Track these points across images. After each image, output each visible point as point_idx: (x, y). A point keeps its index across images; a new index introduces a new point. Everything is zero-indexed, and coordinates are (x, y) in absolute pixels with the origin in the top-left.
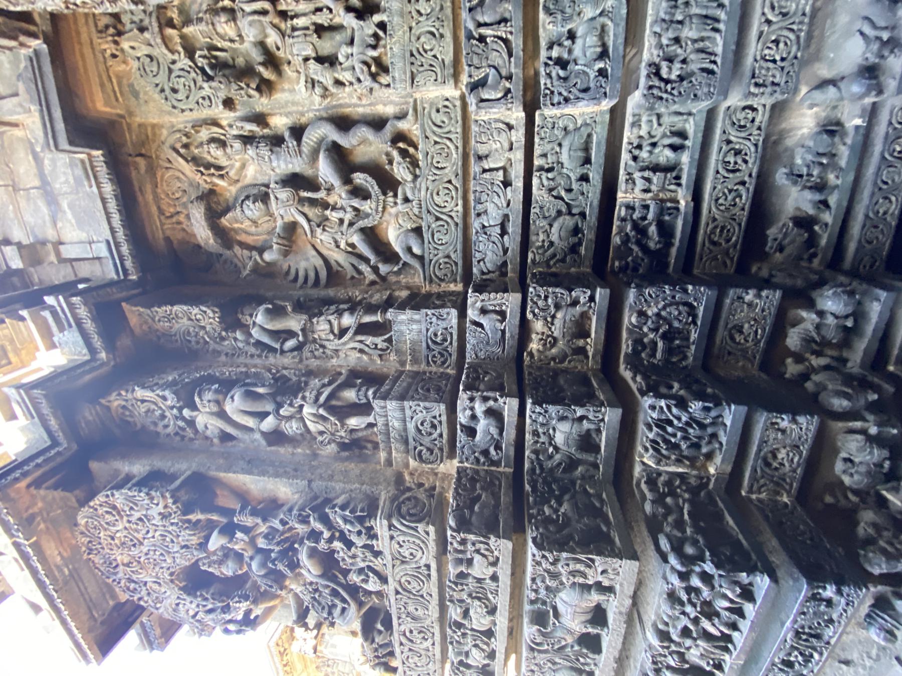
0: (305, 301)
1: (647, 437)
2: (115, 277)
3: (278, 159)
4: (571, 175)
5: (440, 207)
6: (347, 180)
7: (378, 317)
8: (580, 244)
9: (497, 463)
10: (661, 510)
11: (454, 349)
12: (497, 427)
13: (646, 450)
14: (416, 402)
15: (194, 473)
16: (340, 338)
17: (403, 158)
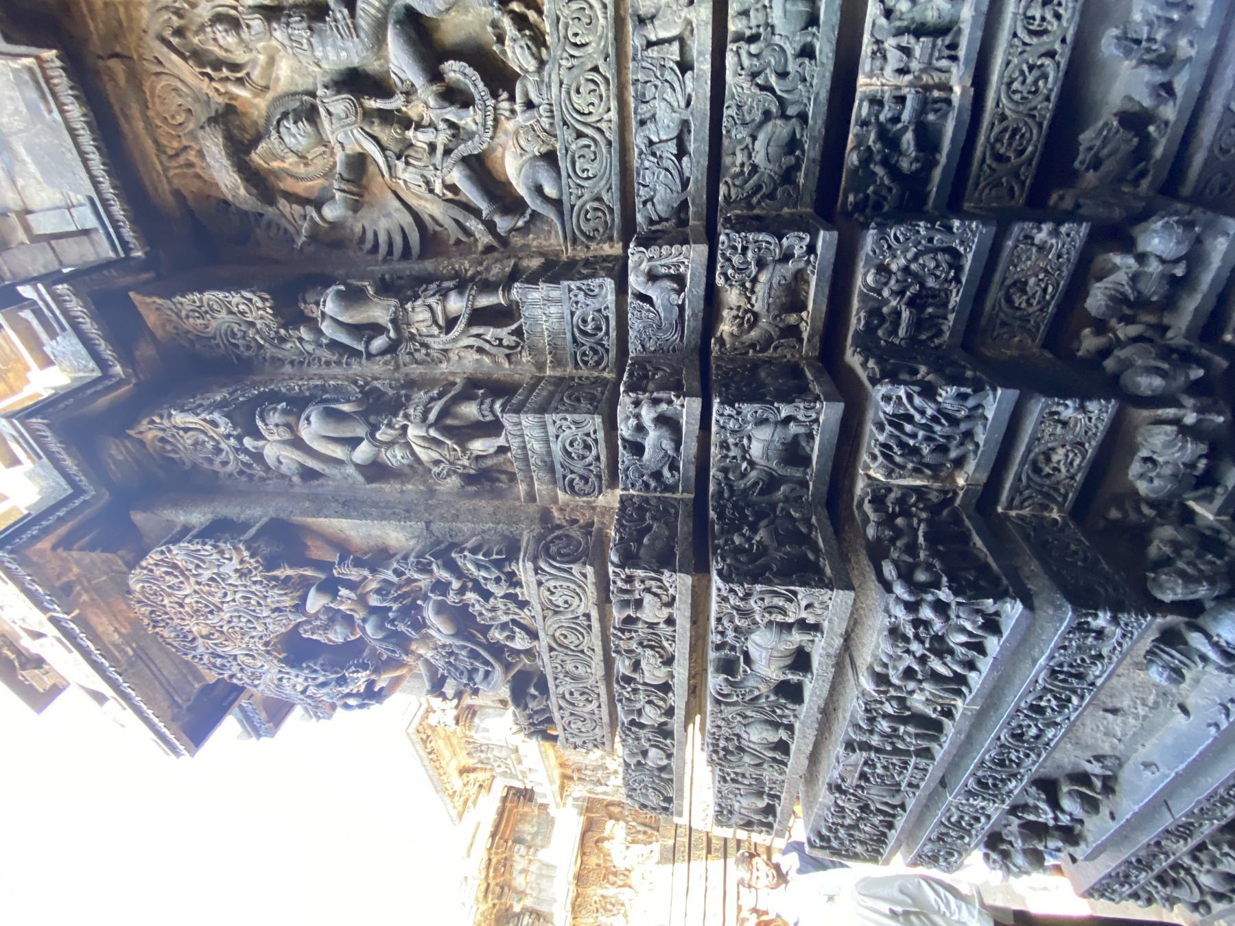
0: (392, 280)
1: (877, 440)
2: (112, 255)
3: (323, 45)
4: (787, 46)
5: (583, 114)
6: (435, 76)
7: (498, 299)
8: (796, 167)
9: (672, 488)
10: (888, 533)
11: (611, 341)
12: (672, 440)
13: (874, 458)
14: (561, 415)
15: (272, 520)
16: (447, 333)
17: (520, 30)
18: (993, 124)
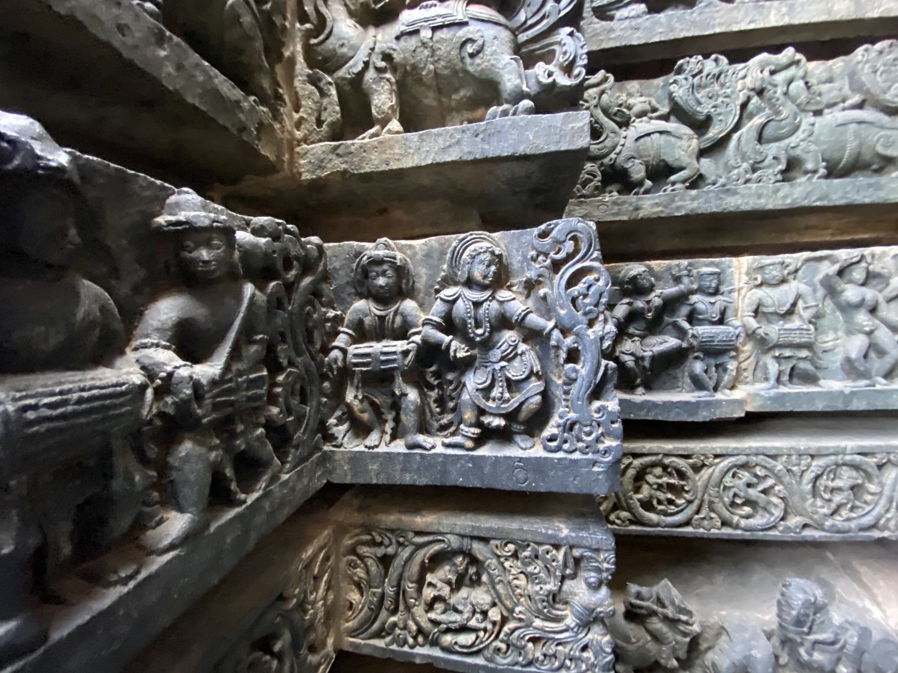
4: (800, 135)
18: (687, 457)
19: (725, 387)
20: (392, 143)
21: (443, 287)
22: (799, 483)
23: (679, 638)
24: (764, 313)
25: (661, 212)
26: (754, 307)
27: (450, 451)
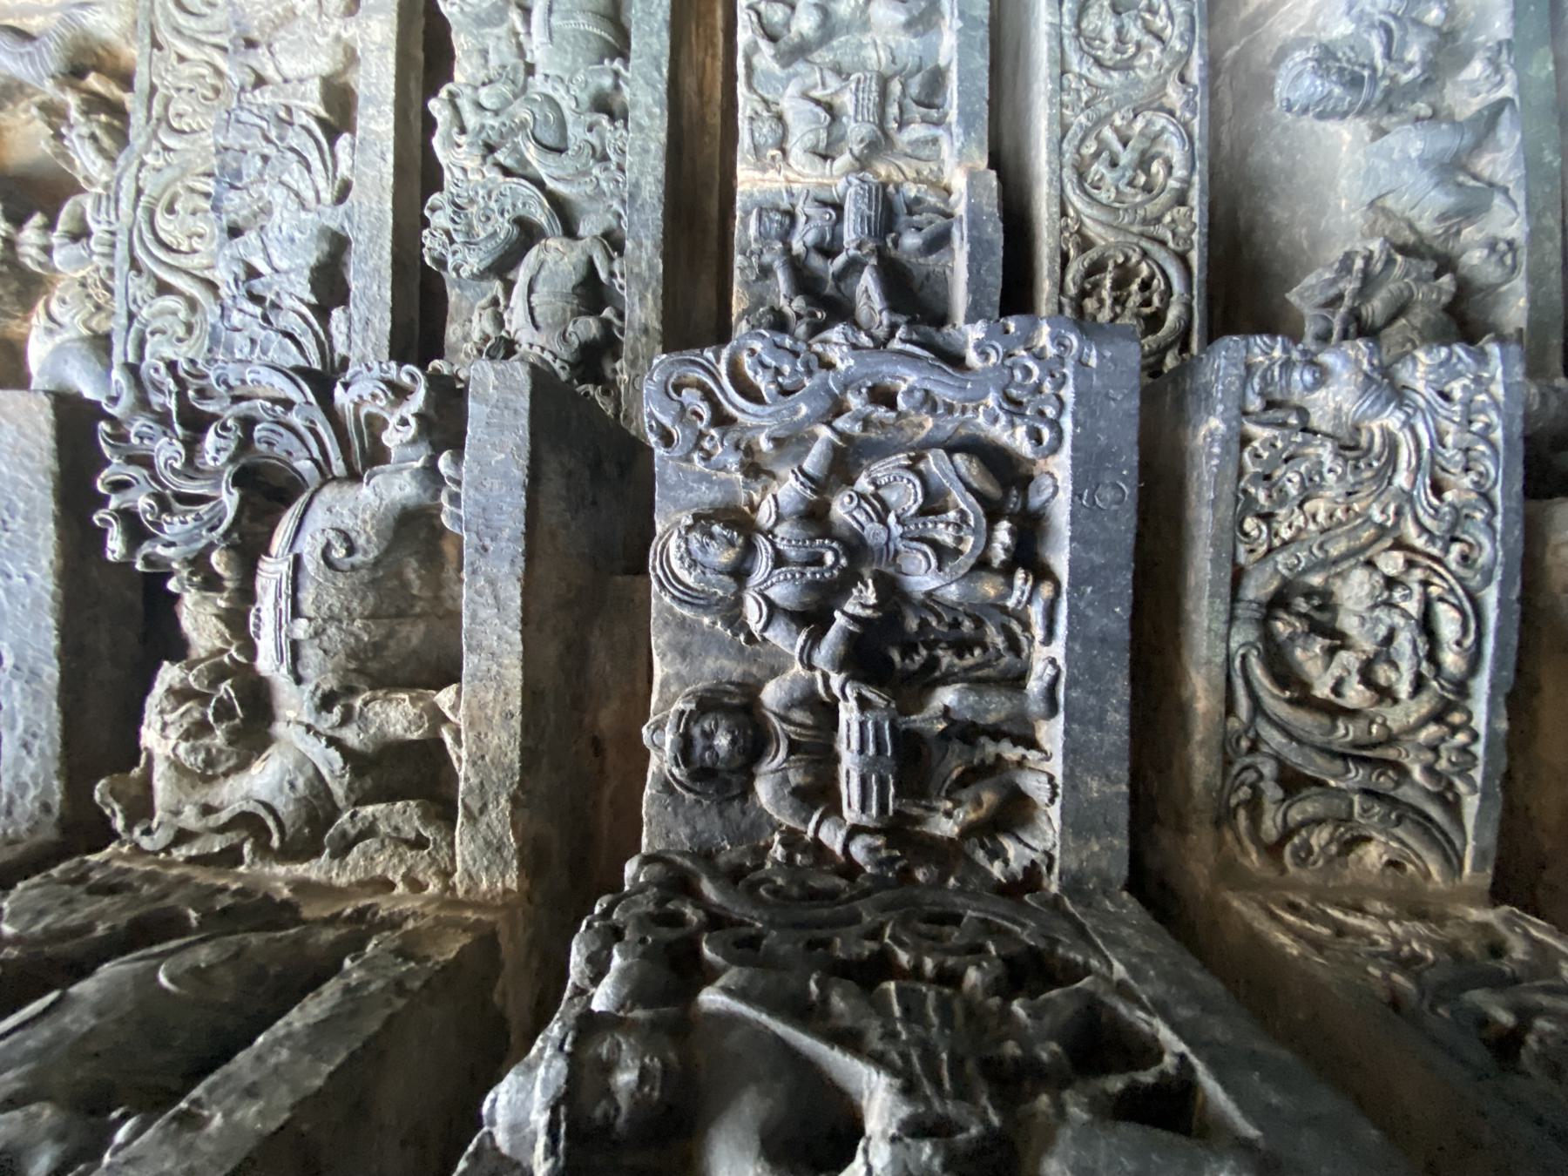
4: (560, 95)
19: (946, 201)
20: (474, 703)
21: (744, 626)
22: (1109, 90)
23: (1397, 271)
24: (828, 145)
25: (654, 293)
26: (817, 159)
27: (1062, 629)
